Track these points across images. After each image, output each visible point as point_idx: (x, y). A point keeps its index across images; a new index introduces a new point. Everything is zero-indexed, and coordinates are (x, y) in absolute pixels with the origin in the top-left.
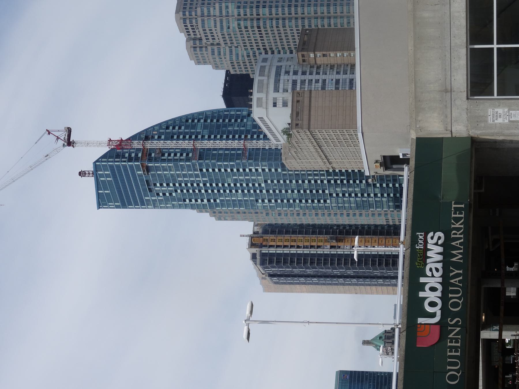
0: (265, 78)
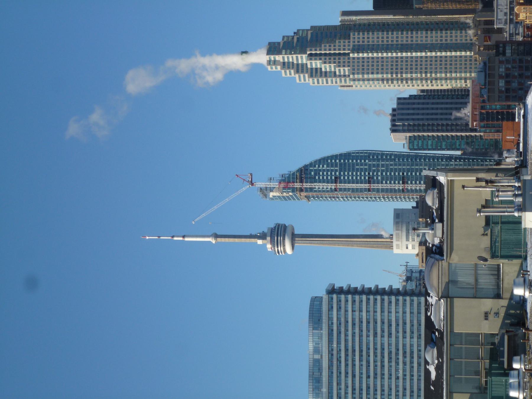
0: (400, 232)
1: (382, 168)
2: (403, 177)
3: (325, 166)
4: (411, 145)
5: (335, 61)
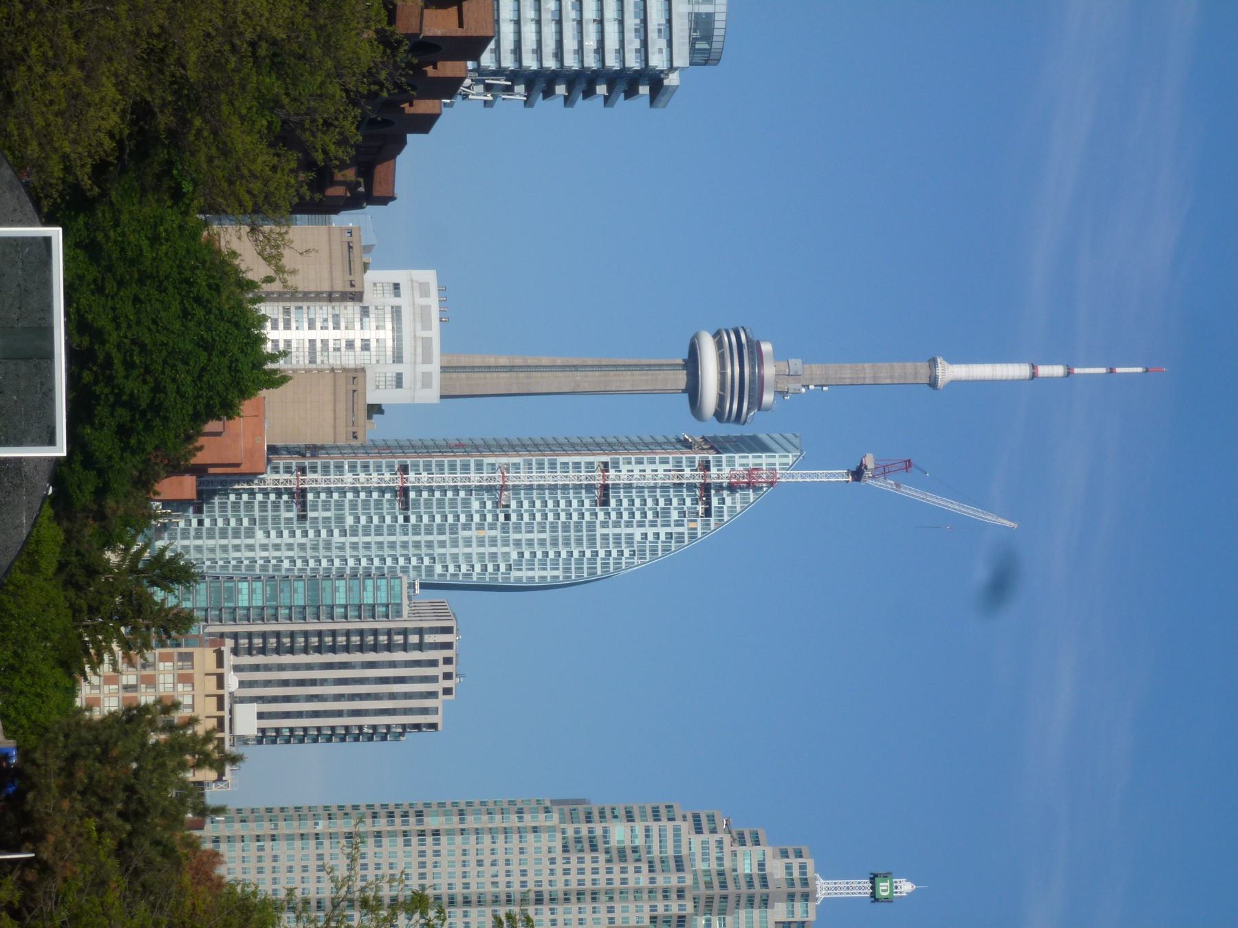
0: (422, 334)
1: (467, 533)
2: (407, 509)
3: (638, 538)
4: (397, 588)
5: (609, 876)
